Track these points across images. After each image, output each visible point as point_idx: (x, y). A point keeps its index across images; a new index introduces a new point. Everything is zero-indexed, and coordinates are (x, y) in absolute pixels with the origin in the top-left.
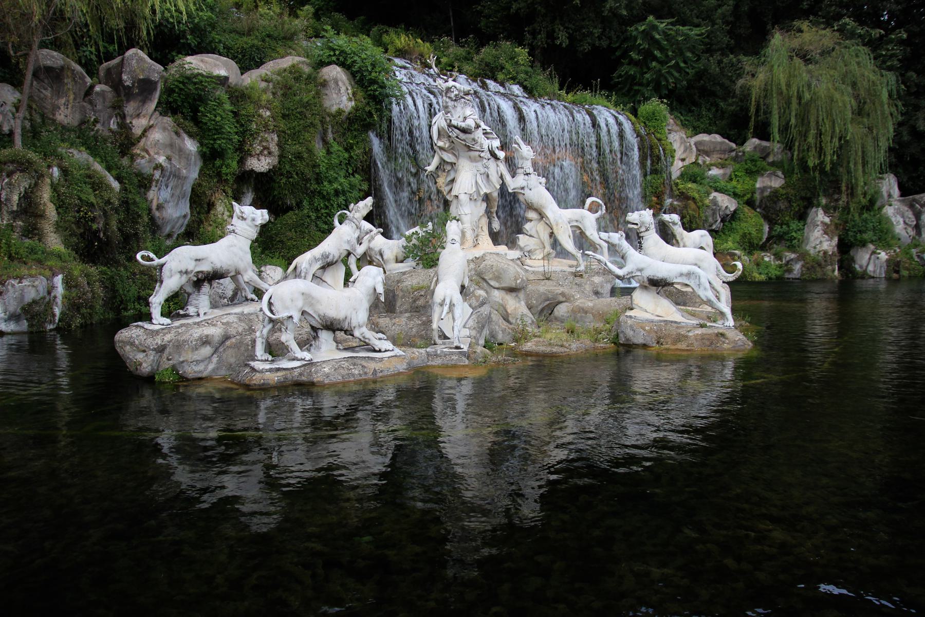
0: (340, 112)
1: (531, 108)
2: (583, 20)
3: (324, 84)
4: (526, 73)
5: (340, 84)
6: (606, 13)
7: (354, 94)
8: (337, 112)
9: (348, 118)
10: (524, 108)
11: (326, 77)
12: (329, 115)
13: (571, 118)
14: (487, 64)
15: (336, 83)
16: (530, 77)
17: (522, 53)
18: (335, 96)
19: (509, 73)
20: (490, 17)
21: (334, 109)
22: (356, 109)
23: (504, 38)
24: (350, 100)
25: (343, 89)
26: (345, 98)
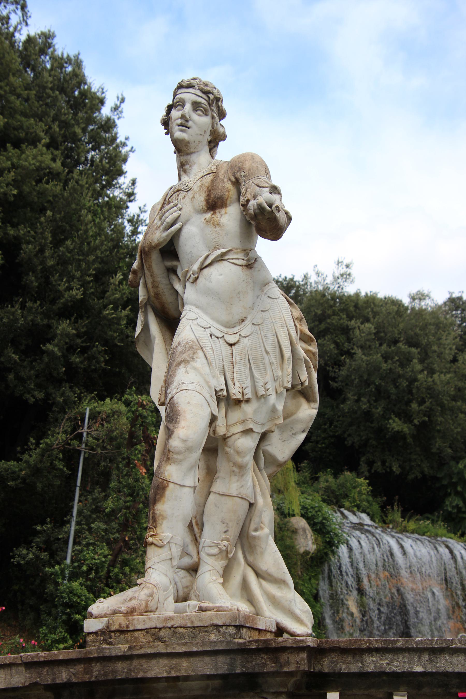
0: (307, 553)
1: (408, 543)
2: (411, 453)
3: (295, 532)
4: (368, 501)
5: (307, 532)
6: (434, 450)
7: (316, 540)
8: (304, 553)
9: (312, 558)
10: (403, 544)
11: (296, 526)
12: (299, 554)
13: (436, 552)
14: (333, 492)
15: (304, 530)
16: (371, 505)
17: (363, 483)
18: (302, 540)
19: (354, 501)
20: (317, 442)
21: (302, 550)
22: (318, 550)
23: (347, 469)
24: (313, 543)
25: (309, 536)
26: (310, 543)
